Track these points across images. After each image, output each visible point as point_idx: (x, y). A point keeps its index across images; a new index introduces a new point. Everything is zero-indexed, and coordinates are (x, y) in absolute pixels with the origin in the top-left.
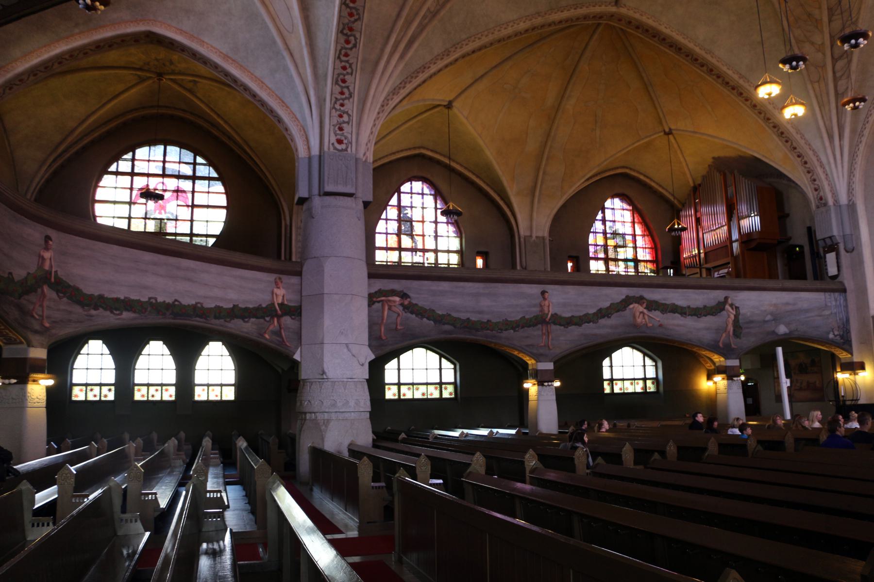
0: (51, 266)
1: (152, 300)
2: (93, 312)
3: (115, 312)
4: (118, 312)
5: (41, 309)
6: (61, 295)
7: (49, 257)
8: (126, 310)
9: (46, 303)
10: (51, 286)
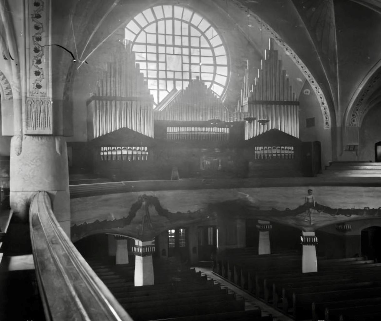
0: (313, 201)
1: (366, 209)
2: (336, 216)
3: (347, 215)
4: (349, 215)
5: (309, 218)
6: (319, 211)
7: (311, 197)
8: (354, 214)
9: (312, 215)
10: (314, 208)
